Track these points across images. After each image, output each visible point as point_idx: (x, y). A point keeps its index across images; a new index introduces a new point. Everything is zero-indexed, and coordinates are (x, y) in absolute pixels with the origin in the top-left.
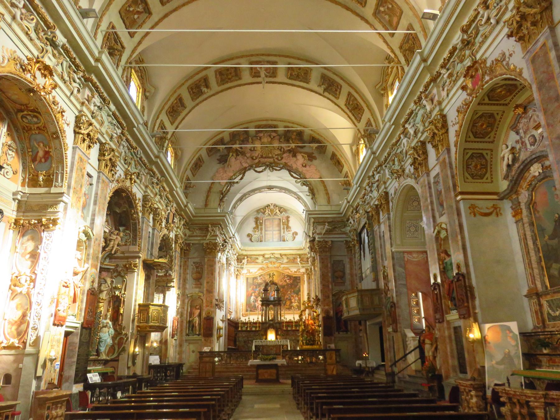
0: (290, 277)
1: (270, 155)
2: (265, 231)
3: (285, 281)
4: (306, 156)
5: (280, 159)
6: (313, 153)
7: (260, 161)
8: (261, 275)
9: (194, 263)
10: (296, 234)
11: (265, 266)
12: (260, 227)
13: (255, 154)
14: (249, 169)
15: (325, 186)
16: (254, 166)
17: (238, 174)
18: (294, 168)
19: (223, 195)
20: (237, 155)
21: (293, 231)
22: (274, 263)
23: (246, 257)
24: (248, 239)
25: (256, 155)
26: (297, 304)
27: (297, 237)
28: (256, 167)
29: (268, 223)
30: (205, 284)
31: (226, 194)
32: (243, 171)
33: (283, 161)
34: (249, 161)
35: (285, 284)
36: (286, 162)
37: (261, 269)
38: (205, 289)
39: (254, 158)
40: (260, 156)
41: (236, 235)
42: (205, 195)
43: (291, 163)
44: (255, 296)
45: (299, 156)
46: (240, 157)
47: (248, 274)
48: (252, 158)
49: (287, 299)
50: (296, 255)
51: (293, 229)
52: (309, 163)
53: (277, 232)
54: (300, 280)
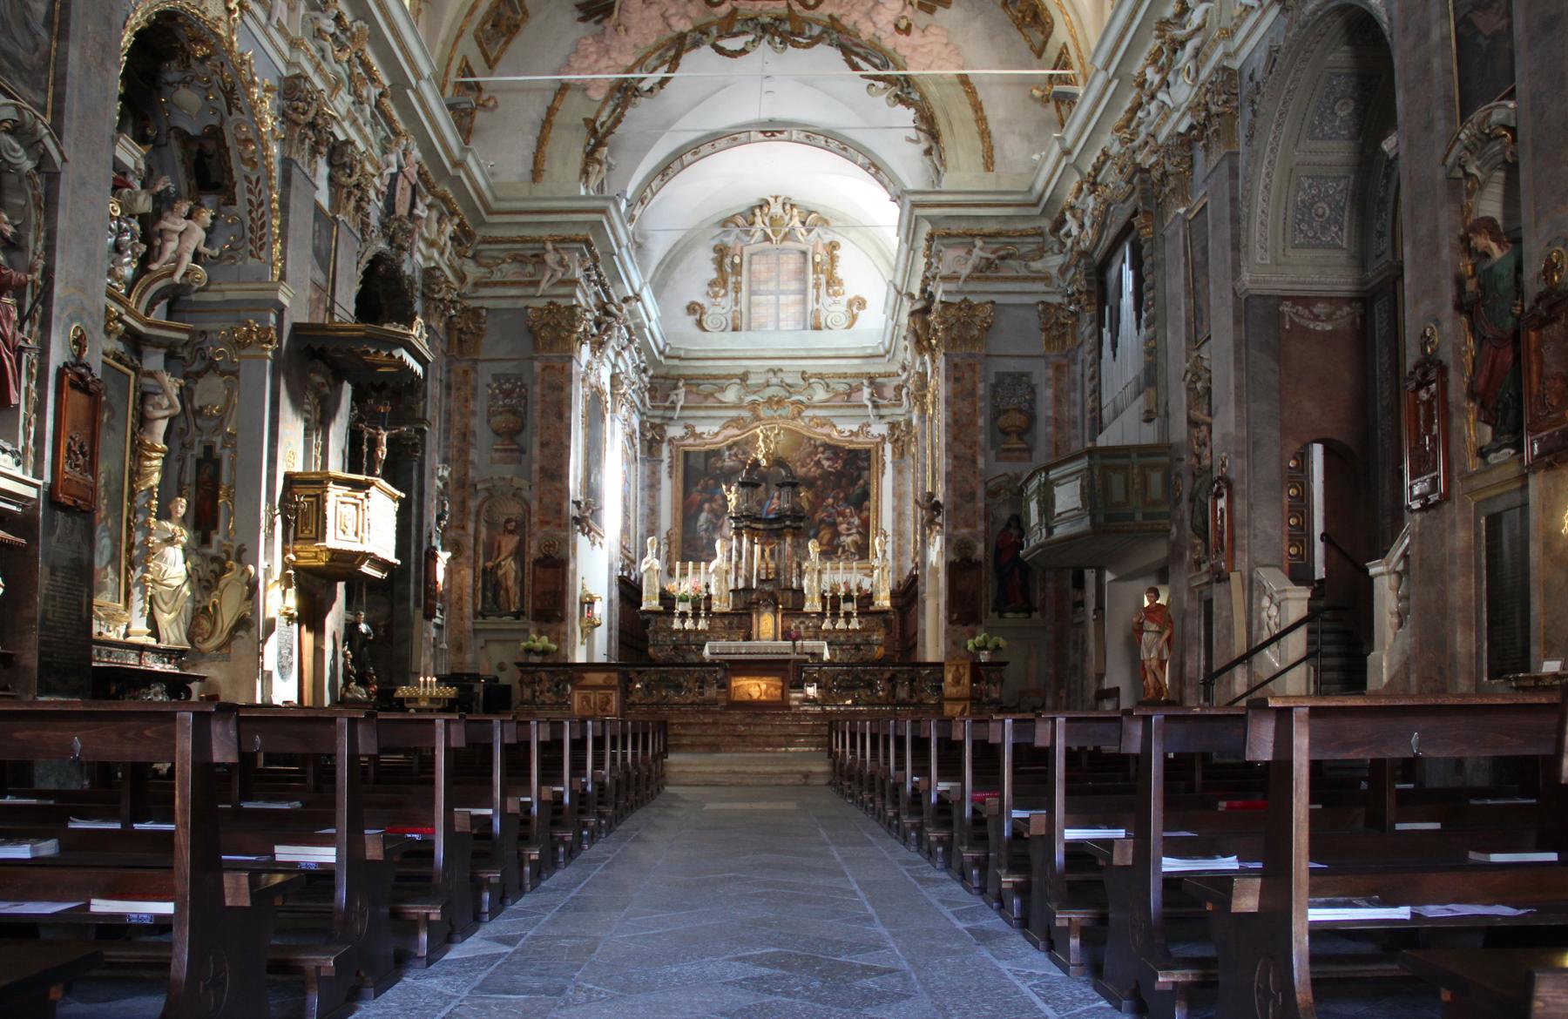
0: (834, 450)
2: (752, 293)
3: (818, 464)
7: (735, 10)
8: (735, 444)
9: (496, 377)
10: (862, 304)
11: (746, 414)
12: (731, 279)
14: (696, 44)
15: (977, 107)
16: (714, 31)
17: (652, 61)
19: (598, 138)
21: (850, 295)
22: (780, 402)
23: (681, 384)
24: (692, 319)
26: (856, 537)
27: (862, 314)
28: (720, 37)
29: (760, 267)
30: (536, 451)
31: (609, 132)
32: (675, 49)
35: (815, 472)
36: (836, 13)
37: (734, 422)
38: (536, 467)
41: (647, 295)
42: (532, 141)
43: (855, 16)
44: (712, 511)
47: (691, 441)
49: (822, 521)
50: (857, 376)
51: (851, 289)
52: (922, 18)
53: (792, 298)
54: (868, 459)
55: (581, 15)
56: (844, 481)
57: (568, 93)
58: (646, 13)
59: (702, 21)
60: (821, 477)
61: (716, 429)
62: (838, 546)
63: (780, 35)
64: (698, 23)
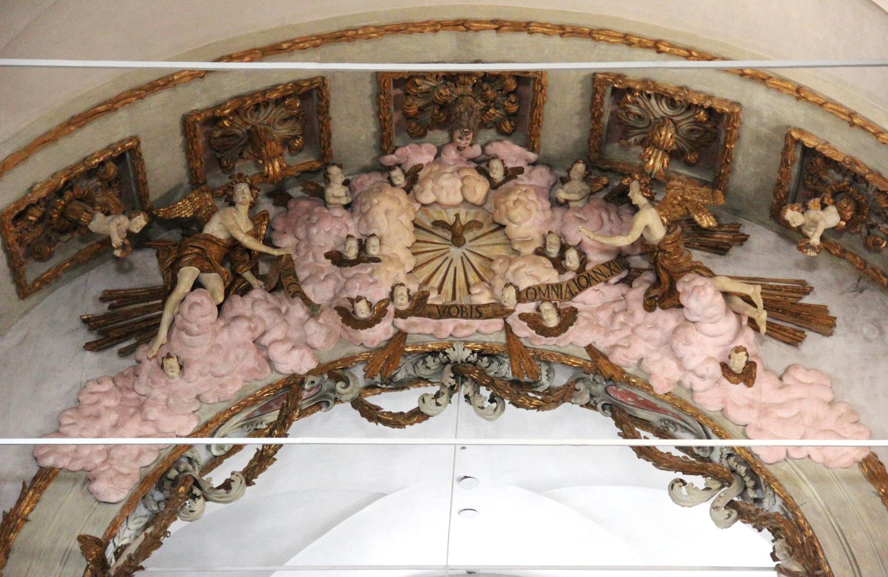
1: (482, 297)
4: (755, 292)
5: (552, 320)
6: (804, 289)
7: (401, 336)
13: (371, 286)
14: (322, 402)
18: (660, 387)
20: (236, 287)
25: (379, 294)
28: (372, 388)
33: (577, 339)
34: (316, 333)
36: (602, 345)
39: (362, 310)
40: (403, 303)
43: (640, 349)
45: (701, 297)
46: (256, 305)
48: (348, 316)
52: (774, 354)
55: (92, 338)
57: (52, 486)
58: (224, 336)
59: (332, 352)
63: (491, 383)
64: (326, 359)
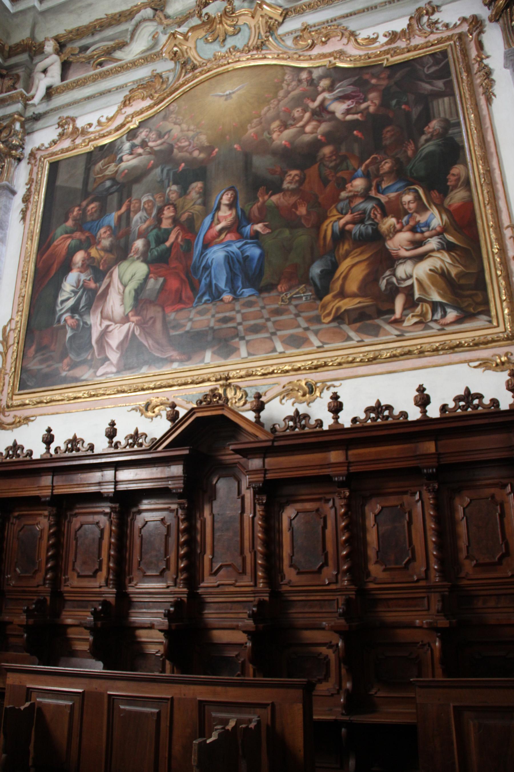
0: (358, 79)
3: (322, 112)
11: (165, 67)
26: (441, 260)
35: (313, 130)
37: (145, 87)
44: (90, 265)
49: (342, 235)
54: (444, 73)
56: (388, 134)
60: (330, 137)
61: (111, 112)
62: (393, 291)
